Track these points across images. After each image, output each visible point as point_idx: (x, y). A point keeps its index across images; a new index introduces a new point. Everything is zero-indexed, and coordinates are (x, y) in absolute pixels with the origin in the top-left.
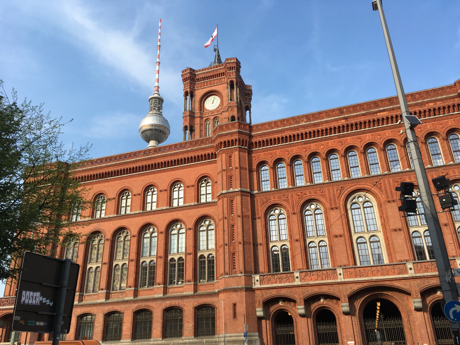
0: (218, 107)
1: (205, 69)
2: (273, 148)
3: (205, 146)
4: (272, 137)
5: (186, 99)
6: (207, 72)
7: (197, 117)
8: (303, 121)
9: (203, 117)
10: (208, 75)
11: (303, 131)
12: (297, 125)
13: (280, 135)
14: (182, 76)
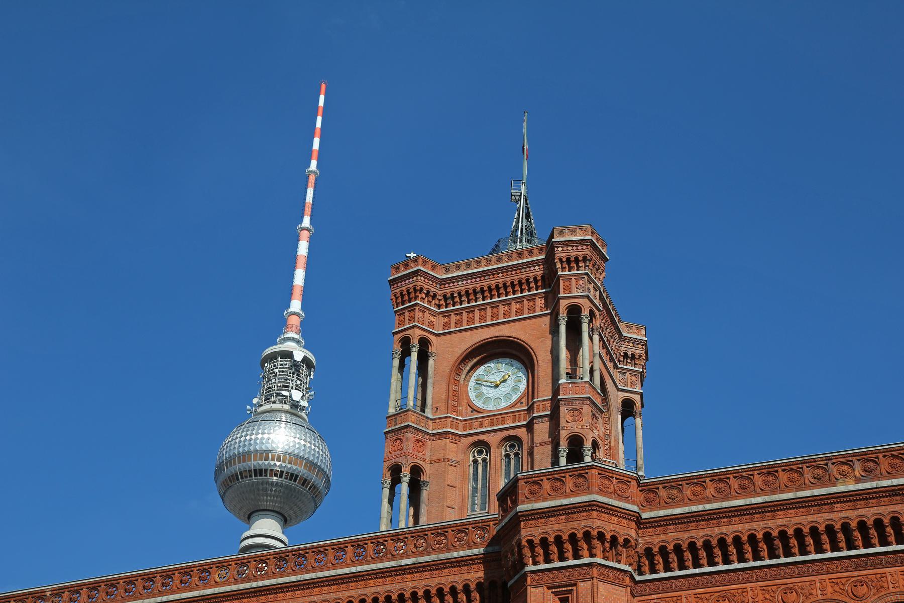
0: (519, 401)
3: (468, 552)
8: (844, 475)
13: (758, 526)
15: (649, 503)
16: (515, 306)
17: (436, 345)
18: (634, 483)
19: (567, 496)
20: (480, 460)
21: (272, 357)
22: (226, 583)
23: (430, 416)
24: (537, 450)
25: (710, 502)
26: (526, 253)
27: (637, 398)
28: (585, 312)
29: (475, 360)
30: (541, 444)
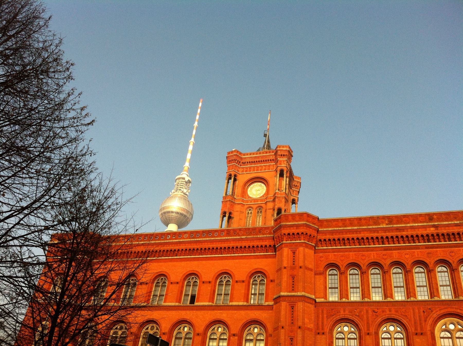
0: (263, 196)
1: (254, 154)
3: (263, 236)
4: (346, 236)
5: (228, 182)
7: (239, 204)
9: (244, 205)
10: (255, 160)
11: (384, 235)
12: (376, 227)
13: (355, 236)
14: (227, 157)
15: (321, 226)
19: (297, 221)
21: (179, 178)
22: (187, 238)
24: (268, 211)
25: (340, 227)
27: (296, 199)
30: (269, 209)
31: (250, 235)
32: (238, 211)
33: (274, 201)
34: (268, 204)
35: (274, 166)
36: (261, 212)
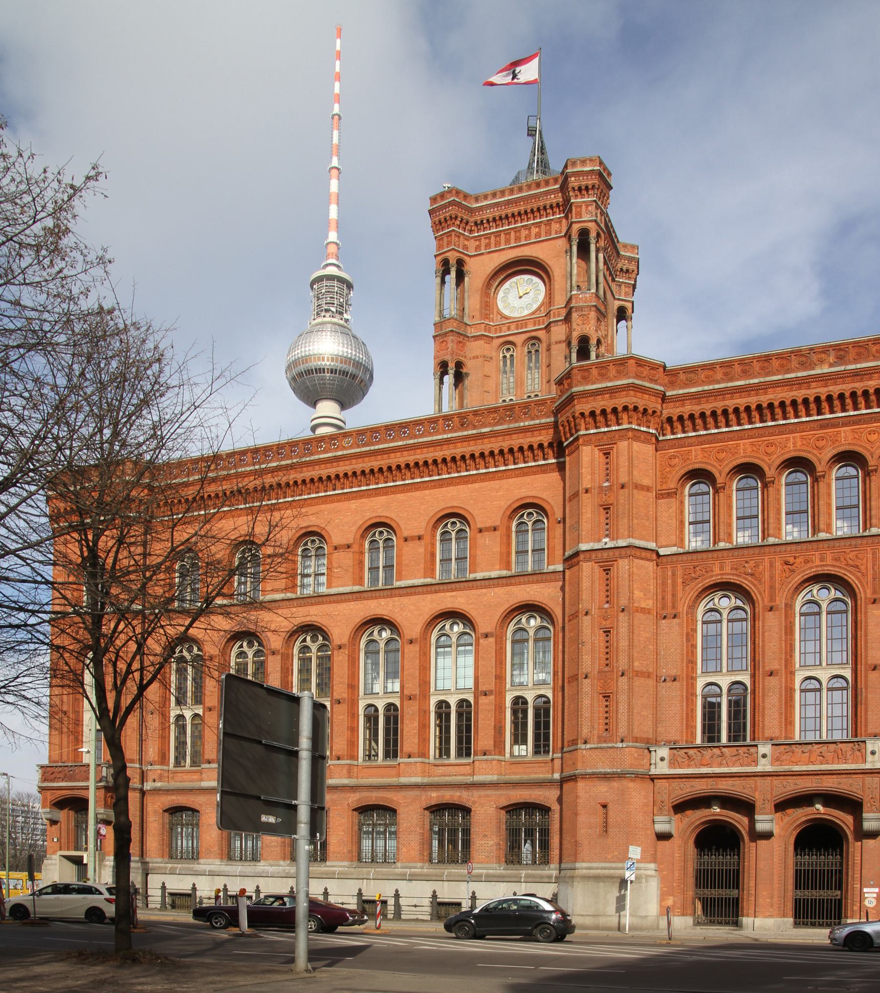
0: (539, 309)
1: (503, 193)
2: (730, 435)
3: (532, 423)
4: (731, 403)
6: (509, 202)
8: (822, 361)
9: (492, 338)
10: (509, 211)
11: (823, 392)
12: (805, 374)
13: (753, 401)
15: (672, 384)
16: (534, 230)
17: (471, 265)
18: (661, 369)
19: (611, 380)
20: (508, 356)
22: (351, 447)
23: (468, 323)
24: (553, 347)
25: (718, 382)
26: (543, 184)
27: (629, 305)
28: (593, 235)
29: (502, 277)
30: (556, 343)
31: (502, 424)
32: (477, 357)
33: (568, 319)
34: (554, 329)
35: (560, 222)
36: (537, 351)
